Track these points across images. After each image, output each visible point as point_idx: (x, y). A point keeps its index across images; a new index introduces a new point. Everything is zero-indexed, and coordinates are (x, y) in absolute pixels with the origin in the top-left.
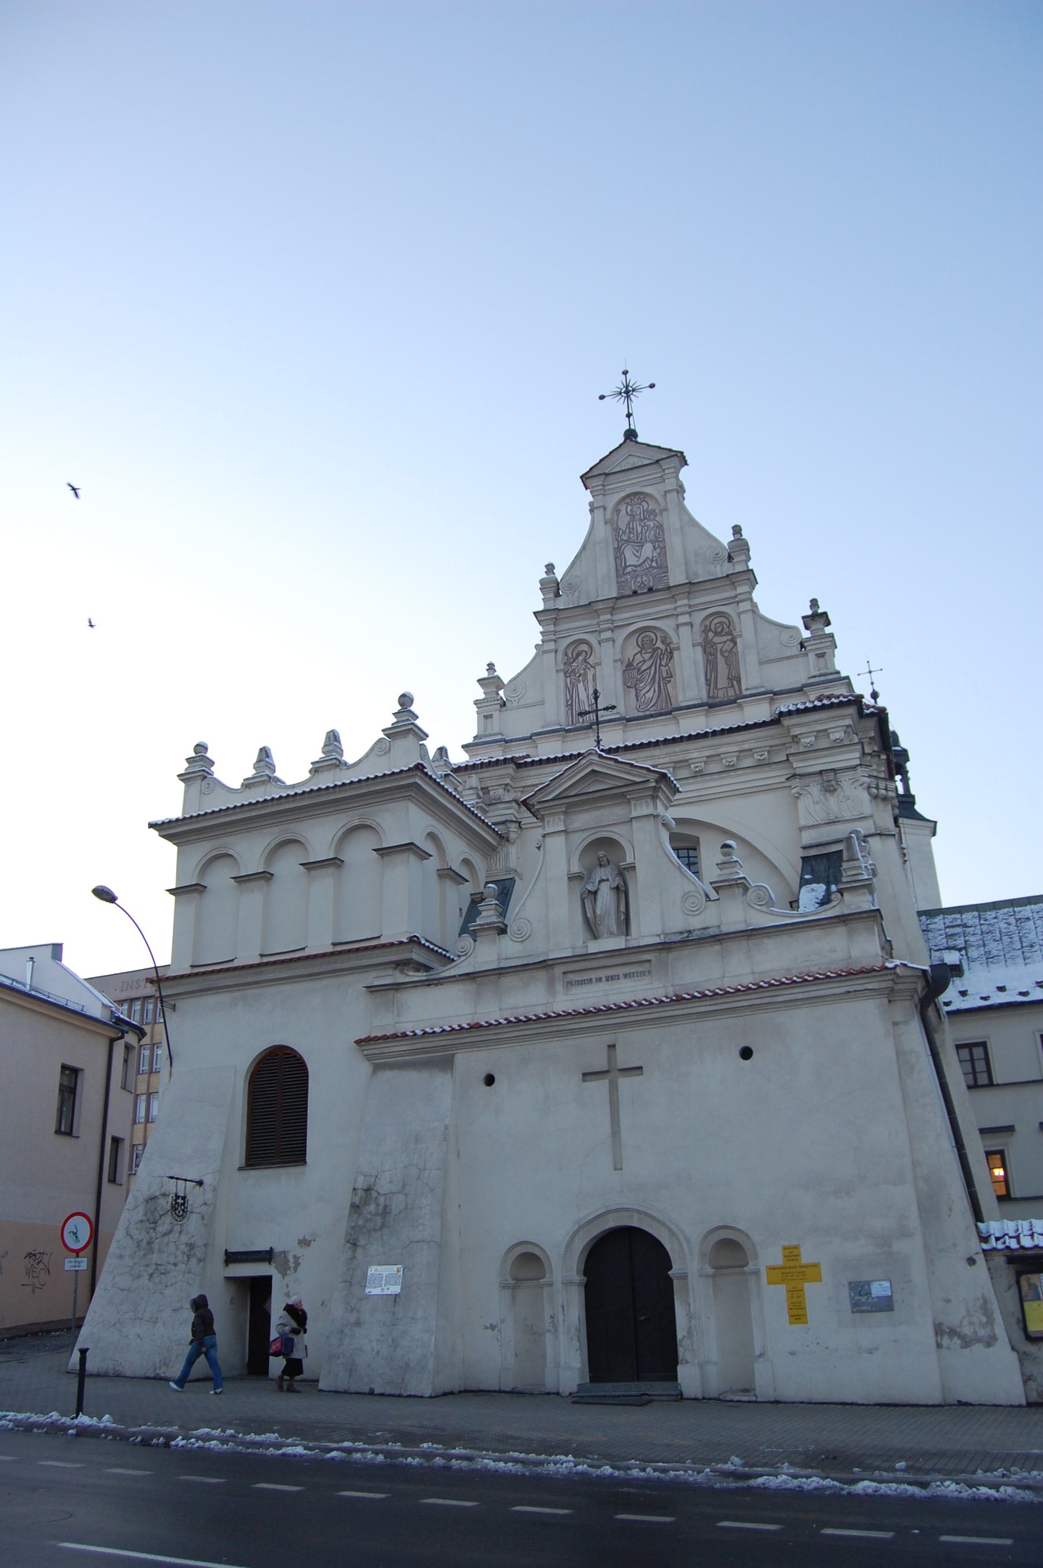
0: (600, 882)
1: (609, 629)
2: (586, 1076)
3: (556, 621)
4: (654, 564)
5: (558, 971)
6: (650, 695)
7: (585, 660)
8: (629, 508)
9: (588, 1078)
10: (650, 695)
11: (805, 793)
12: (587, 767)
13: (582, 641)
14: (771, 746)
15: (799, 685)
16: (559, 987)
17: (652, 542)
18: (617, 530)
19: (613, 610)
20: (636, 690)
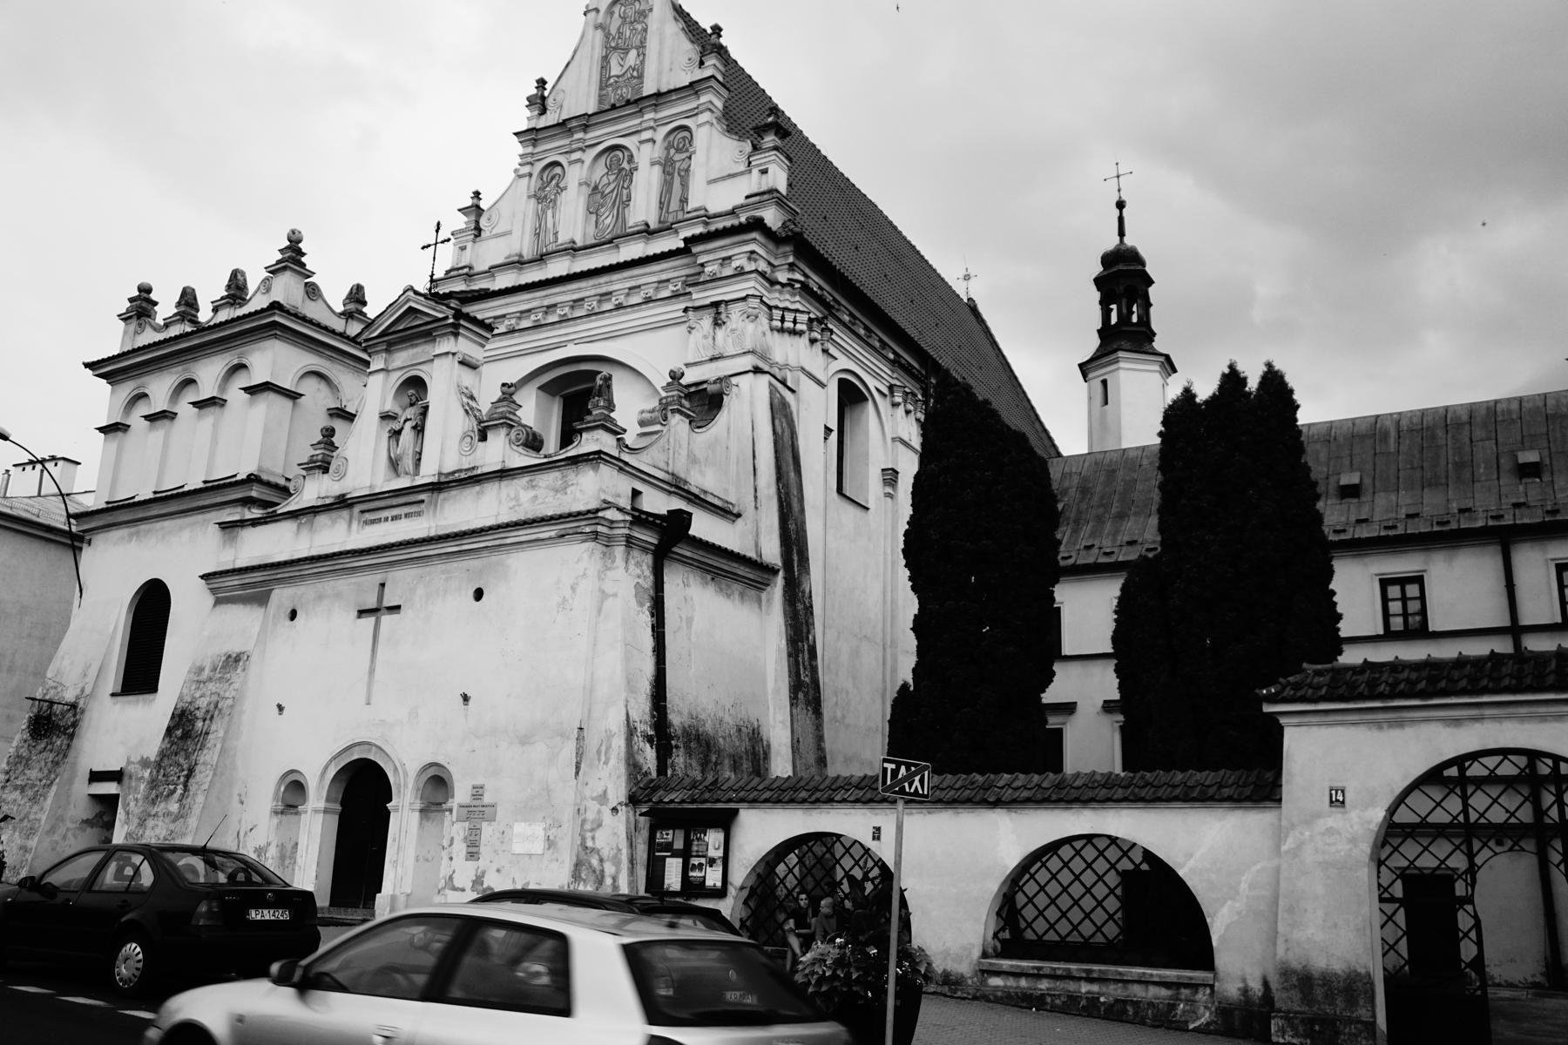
0: (405, 421)
1: (580, 149)
2: (362, 613)
3: (535, 142)
4: (635, 74)
5: (357, 509)
6: (608, 221)
7: (557, 185)
8: (623, 8)
9: (363, 615)
10: (608, 221)
11: (698, 326)
12: (405, 303)
13: (556, 164)
14: (687, 276)
15: (730, 207)
16: (355, 525)
17: (637, 48)
18: (607, 35)
19: (585, 128)
20: (597, 215)
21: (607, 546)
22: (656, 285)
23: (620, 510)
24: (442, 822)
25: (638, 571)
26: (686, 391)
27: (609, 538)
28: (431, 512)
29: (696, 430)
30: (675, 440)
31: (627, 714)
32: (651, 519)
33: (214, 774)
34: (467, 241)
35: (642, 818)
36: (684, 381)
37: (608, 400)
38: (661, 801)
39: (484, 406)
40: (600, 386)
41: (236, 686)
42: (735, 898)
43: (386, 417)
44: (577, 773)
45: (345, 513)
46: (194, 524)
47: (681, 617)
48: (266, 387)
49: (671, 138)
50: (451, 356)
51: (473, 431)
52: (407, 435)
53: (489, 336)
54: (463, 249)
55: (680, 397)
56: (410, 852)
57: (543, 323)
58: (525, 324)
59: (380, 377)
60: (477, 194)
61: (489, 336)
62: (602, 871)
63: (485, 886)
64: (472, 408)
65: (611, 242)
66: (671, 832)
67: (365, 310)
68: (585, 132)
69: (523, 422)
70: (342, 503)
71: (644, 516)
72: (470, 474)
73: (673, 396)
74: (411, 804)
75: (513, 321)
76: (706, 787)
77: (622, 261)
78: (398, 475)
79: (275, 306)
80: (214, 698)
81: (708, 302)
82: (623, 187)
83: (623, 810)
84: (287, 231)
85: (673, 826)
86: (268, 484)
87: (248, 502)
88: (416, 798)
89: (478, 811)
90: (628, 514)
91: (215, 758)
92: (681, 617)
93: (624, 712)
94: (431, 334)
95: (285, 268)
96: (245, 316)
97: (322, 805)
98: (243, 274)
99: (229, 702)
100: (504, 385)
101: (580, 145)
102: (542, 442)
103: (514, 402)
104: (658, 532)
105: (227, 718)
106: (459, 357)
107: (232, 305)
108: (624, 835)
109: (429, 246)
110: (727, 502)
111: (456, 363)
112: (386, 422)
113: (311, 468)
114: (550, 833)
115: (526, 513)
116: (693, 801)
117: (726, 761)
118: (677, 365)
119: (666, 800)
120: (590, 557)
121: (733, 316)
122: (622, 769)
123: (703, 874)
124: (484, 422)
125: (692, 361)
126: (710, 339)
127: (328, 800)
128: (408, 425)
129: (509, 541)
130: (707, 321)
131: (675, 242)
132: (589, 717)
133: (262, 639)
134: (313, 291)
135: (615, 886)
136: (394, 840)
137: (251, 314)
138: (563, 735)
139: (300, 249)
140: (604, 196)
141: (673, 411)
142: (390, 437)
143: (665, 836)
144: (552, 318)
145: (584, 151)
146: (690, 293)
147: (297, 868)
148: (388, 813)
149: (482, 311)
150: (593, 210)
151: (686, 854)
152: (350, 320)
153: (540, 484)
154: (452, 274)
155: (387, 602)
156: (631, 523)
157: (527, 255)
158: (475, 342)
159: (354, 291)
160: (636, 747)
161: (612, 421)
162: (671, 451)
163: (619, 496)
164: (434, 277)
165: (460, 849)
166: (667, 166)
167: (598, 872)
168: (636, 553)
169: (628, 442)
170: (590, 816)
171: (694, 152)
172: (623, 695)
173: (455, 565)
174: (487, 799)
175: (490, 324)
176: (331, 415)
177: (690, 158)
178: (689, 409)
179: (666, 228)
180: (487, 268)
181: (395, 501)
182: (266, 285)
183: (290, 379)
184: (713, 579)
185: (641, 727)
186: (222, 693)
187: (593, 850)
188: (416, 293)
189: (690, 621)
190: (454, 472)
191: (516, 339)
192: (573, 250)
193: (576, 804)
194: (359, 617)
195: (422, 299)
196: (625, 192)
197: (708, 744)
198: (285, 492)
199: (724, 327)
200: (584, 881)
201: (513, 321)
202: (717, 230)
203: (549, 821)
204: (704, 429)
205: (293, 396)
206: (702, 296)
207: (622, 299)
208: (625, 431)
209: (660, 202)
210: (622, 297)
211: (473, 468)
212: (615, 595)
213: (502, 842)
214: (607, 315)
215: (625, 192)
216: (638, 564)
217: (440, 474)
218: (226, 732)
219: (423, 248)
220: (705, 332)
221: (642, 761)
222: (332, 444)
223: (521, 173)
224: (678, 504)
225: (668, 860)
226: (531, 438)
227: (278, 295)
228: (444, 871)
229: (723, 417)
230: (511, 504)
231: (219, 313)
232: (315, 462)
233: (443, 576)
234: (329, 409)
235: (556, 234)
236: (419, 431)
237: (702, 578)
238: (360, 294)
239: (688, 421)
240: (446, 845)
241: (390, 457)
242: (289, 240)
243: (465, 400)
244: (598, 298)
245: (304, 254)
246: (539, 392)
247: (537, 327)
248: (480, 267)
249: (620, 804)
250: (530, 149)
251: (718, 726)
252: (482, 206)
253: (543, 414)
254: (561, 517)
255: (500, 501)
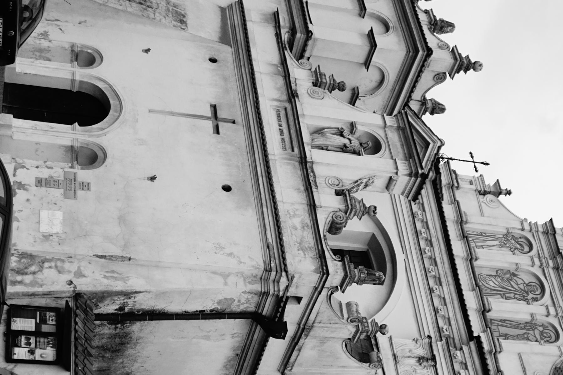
5: (288, 105)
14: (453, 339)
21: (261, 279)
22: (447, 316)
23: (287, 288)
24: (64, 161)
25: (243, 301)
26: (372, 336)
27: (267, 280)
28: (285, 156)
29: (344, 344)
30: (336, 328)
31: (140, 292)
32: (280, 310)
33: (101, 4)
34: (476, 185)
35: (64, 302)
36: (379, 335)
37: (365, 280)
38: (76, 316)
39: (358, 195)
40: (375, 275)
41: (163, 20)
42: (5, 369)
43: (352, 126)
44: (98, 256)
45: (285, 97)
47: (210, 331)
48: (373, 45)
49: (550, 328)
50: (395, 171)
51: (342, 186)
52: (340, 141)
53: (409, 198)
54: (471, 183)
55: (367, 332)
56: (43, 139)
57: (420, 237)
58: (419, 225)
59: (380, 122)
60: (509, 193)
61: (409, 198)
62: (26, 274)
63: (17, 191)
64: (359, 185)
65: (477, 285)
66: (54, 323)
67: (428, 114)
68: (553, 268)
69: (349, 221)
71: (282, 304)
72: (312, 183)
73: (368, 326)
74: (77, 139)
75: (420, 217)
76: (86, 348)
77: (464, 293)
78: (312, 134)
79: (429, 52)
80: (155, 6)
81: (435, 352)
82: (515, 294)
83: (70, 288)
84: (482, 61)
85: (58, 325)
86: (305, 45)
87: (293, 31)
88: (81, 143)
90: (284, 293)
91: (112, 5)
92: (210, 331)
93: (142, 290)
94: (411, 157)
95: (456, 59)
96: (422, 31)
97: (78, 78)
98: (452, 31)
99: (152, 16)
100: (375, 207)
101: (544, 265)
102: (335, 234)
103: (363, 215)
104: (271, 315)
105: (140, 14)
106: (395, 177)
107: (430, 23)
108: (52, 289)
109: (472, 157)
110: (292, 366)
111: (390, 175)
112: (349, 127)
113: (316, 75)
114: (54, 237)
115: (285, 222)
116: (76, 339)
117: (105, 364)
118: (391, 330)
119: (77, 320)
120: (253, 266)
121: (425, 371)
122: (100, 288)
123: (23, 345)
124: (349, 193)
125: (393, 341)
126: (408, 354)
127: (81, 82)
128: (347, 142)
131: (477, 329)
132: (139, 265)
133: (196, 39)
134: (440, 78)
135: (14, 283)
136: (51, 128)
137: (423, 35)
138: (125, 246)
139: (469, 70)
140: (509, 280)
141: (357, 327)
142: (338, 129)
143: (51, 319)
144: (422, 243)
145: (540, 267)
146: (441, 340)
147: (32, 60)
148: (71, 123)
149: (427, 193)
150: (499, 273)
151: (38, 333)
152: (420, 103)
153: (305, 232)
154: (453, 175)
155: (221, 125)
156: (278, 296)
157: (467, 227)
158: (405, 188)
159: (440, 106)
160: (116, 299)
161: (350, 283)
162: (329, 325)
163: (297, 287)
164: (450, 161)
166: (530, 325)
167: (26, 270)
168: (256, 299)
169: (335, 295)
170: (67, 266)
171: (541, 344)
172: (152, 289)
173: (248, 172)
174: (80, 193)
175: (418, 199)
176: (354, 89)
177: (537, 341)
178: (359, 338)
179: (487, 324)
180: (457, 199)
182: (443, 46)
183: (380, 62)
184: (237, 355)
185: (130, 302)
186: (158, 11)
187: (42, 267)
188: (439, 148)
189: (207, 338)
190: (313, 172)
191: (408, 219)
192: (471, 259)
193: (75, 255)
194: (211, 106)
195: (435, 152)
196: (512, 295)
197: (118, 351)
198: (300, 56)
199: (417, 364)
200: (19, 261)
201: (420, 217)
202: (486, 359)
203: (63, 236)
204: (345, 349)
205: (367, 63)
206: (439, 348)
207: (437, 292)
208: (343, 292)
209: (505, 320)
210: (438, 293)
211: (316, 186)
212: (226, 284)
213: (48, 203)
214: (425, 282)
215: (512, 295)
216: (248, 301)
217: (312, 163)
218: (130, 13)
219: (471, 153)
220: (414, 351)
221: (106, 302)
222: (333, 89)
223: (525, 223)
224: (291, 329)
225: (34, 321)
226: (338, 226)
227: (437, 54)
228: (28, 162)
229: (353, 363)
230: (291, 212)
231: (424, 14)
232: (321, 77)
234: (358, 88)
235: (482, 247)
236: (342, 149)
237: (238, 347)
238: (438, 111)
239: (350, 337)
240: (47, 164)
241: (324, 129)
242: (475, 63)
243: (365, 181)
244: (438, 276)
245: (465, 72)
246: (371, 234)
247: (417, 234)
248: (458, 194)
249: (75, 287)
250: (541, 229)
251: (131, 358)
252: (501, 196)
253: (354, 237)
254: (282, 246)
255: (293, 204)
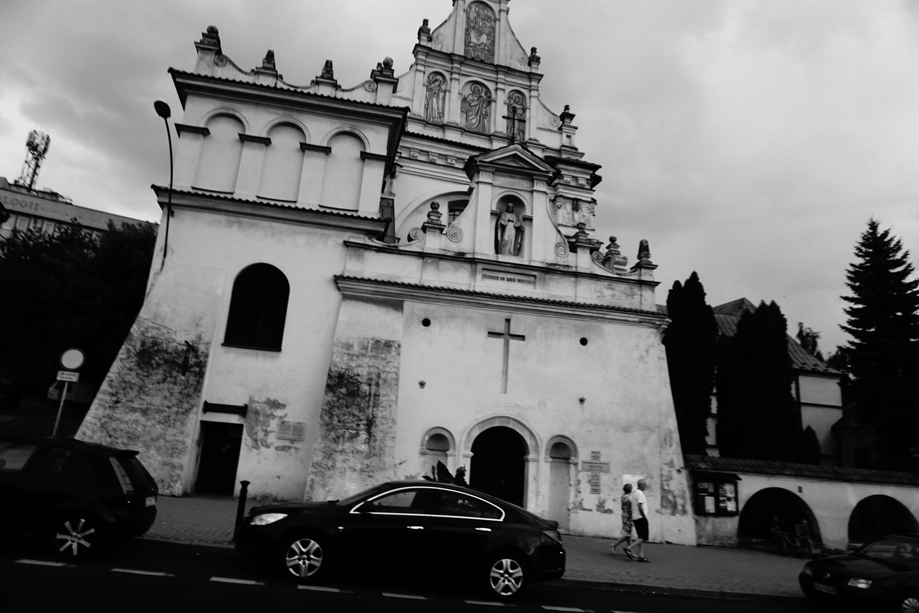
46: (310, 233)
70: (459, 258)
89: (596, 466)
129: (607, 317)
130: (569, 206)
165: (585, 487)
181: (512, 270)
233: (557, 326)
